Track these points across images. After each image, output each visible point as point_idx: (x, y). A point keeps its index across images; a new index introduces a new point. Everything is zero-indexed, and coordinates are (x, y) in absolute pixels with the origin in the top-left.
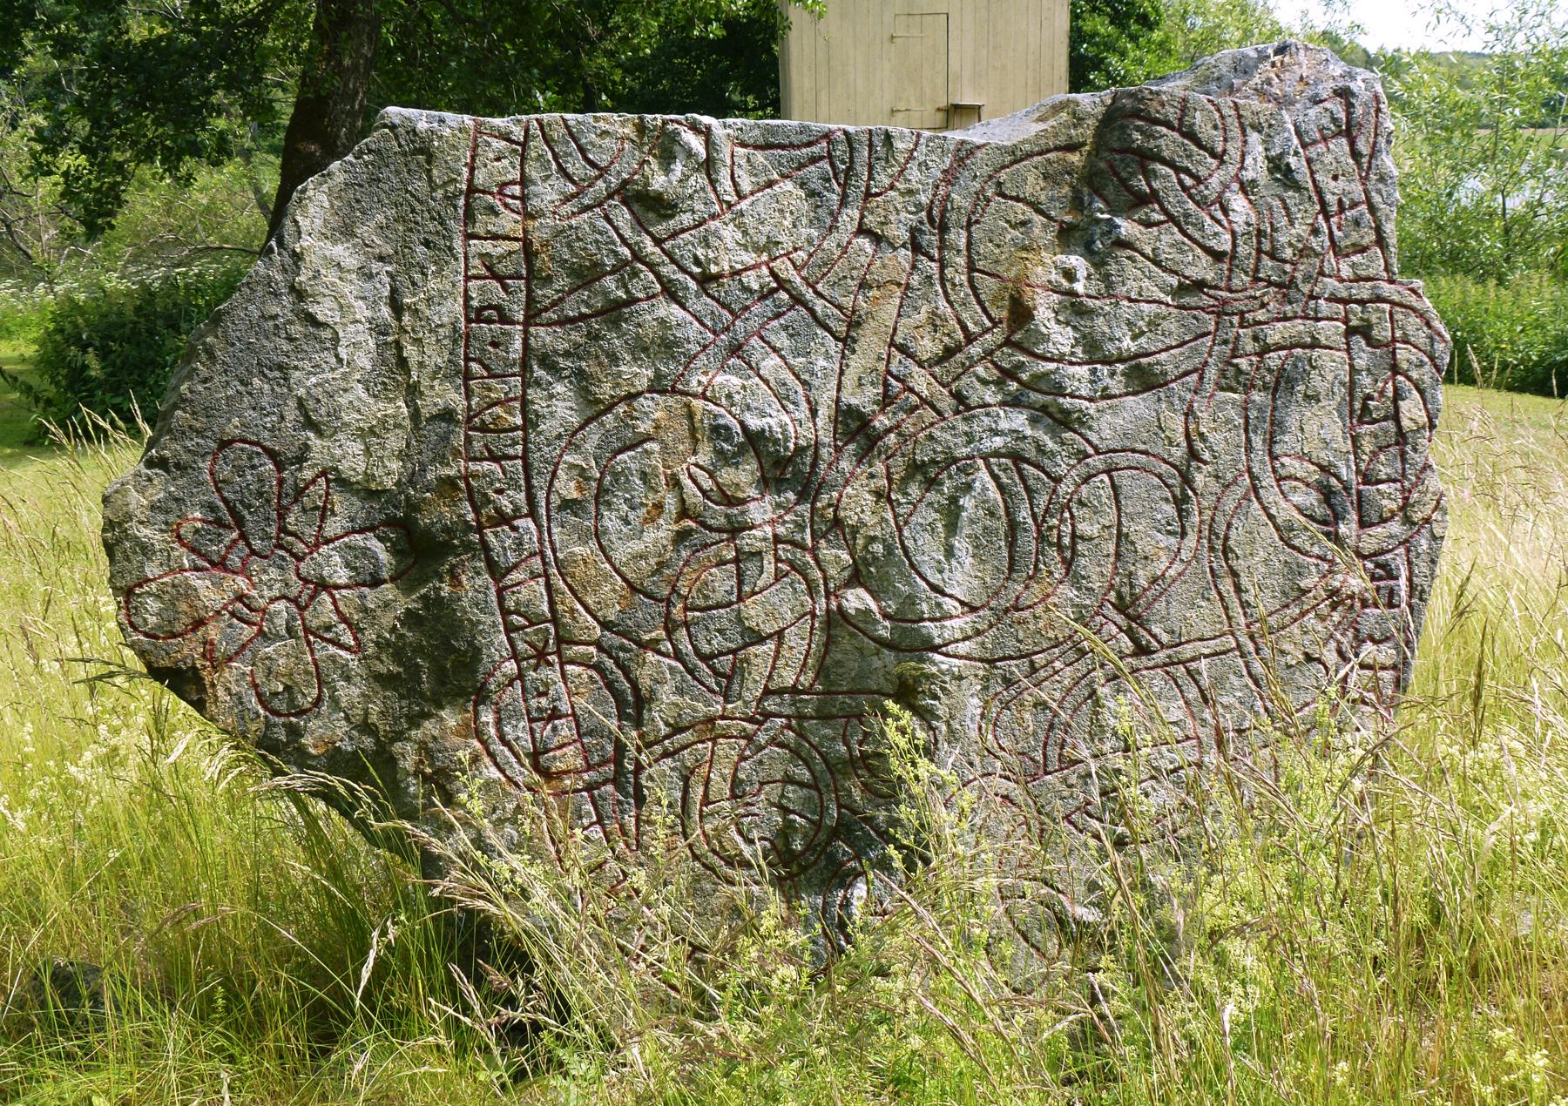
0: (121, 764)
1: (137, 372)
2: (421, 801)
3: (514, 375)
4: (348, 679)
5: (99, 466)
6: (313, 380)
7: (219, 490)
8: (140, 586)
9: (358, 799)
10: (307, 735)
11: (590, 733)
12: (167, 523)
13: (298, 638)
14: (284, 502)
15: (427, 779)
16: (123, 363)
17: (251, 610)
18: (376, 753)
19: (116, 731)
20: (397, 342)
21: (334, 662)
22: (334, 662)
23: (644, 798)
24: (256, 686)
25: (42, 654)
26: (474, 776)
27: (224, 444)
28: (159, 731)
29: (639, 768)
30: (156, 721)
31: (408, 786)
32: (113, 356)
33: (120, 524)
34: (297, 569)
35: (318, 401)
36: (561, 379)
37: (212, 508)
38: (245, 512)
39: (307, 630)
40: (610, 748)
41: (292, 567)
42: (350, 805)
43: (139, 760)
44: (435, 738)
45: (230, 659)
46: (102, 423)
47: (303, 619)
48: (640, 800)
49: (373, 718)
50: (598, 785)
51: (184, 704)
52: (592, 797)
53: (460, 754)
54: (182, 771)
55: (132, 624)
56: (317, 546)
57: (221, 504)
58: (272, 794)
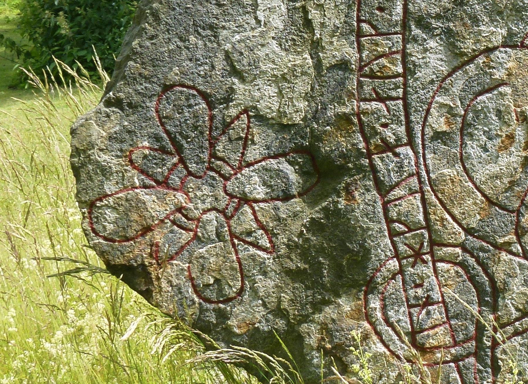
0: (86, 341)
1: (97, 31)
2: (322, 370)
3: (396, 33)
4: (265, 274)
5: (68, 105)
6: (238, 37)
7: (162, 124)
8: (101, 200)
9: (273, 369)
10: (232, 318)
11: (456, 316)
12: (121, 150)
13: (225, 241)
14: (215, 134)
15: (327, 353)
16: (87, 24)
17: (188, 219)
18: (287, 332)
19: (81, 315)
20: (304, 7)
21: (254, 260)
22: (254, 260)
23: (499, 367)
24: (192, 279)
25: (23, 253)
26: (365, 351)
27: (167, 88)
28: (115, 315)
29: (495, 344)
30: (113, 307)
31: (313, 358)
32: (79, 18)
33: (84, 151)
34: (225, 187)
35: (241, 54)
36: (433, 36)
37: (157, 138)
38: (184, 142)
39: (233, 235)
40: (472, 329)
41: (221, 185)
42: (267, 373)
43: (99, 338)
44: (333, 320)
45: (172, 258)
46: (70, 71)
47: (229, 226)
48: (496, 369)
49: (285, 305)
50: (462, 358)
51: (135, 293)
52: (458, 367)
53: (354, 333)
54: (133, 347)
55: (94, 231)
56: (240, 168)
57: (165, 135)
58: (205, 365)
